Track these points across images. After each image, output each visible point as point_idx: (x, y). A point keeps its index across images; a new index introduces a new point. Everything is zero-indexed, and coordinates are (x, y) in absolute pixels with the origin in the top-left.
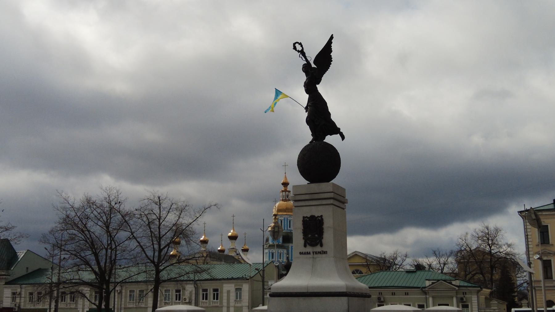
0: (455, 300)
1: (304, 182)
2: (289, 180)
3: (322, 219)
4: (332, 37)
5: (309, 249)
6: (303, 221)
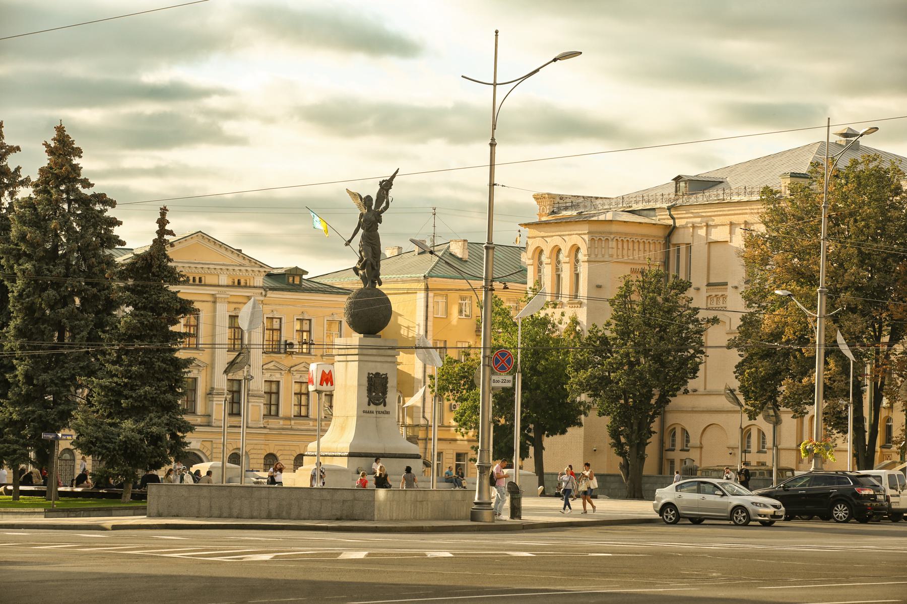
4: (397, 172)
5: (373, 408)
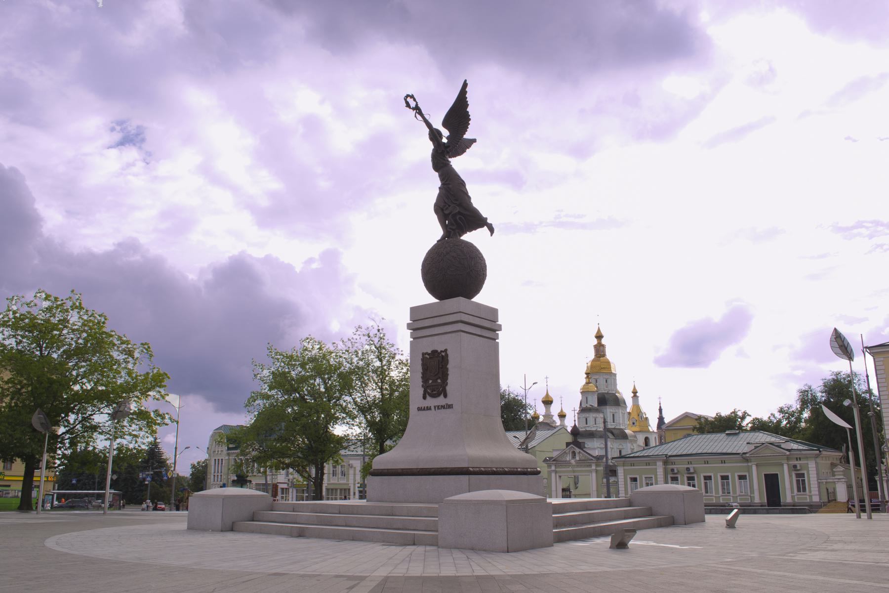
0: (786, 467)
1: (431, 299)
2: (603, 332)
3: (447, 355)
4: (465, 85)
5: (431, 402)
6: (423, 360)
